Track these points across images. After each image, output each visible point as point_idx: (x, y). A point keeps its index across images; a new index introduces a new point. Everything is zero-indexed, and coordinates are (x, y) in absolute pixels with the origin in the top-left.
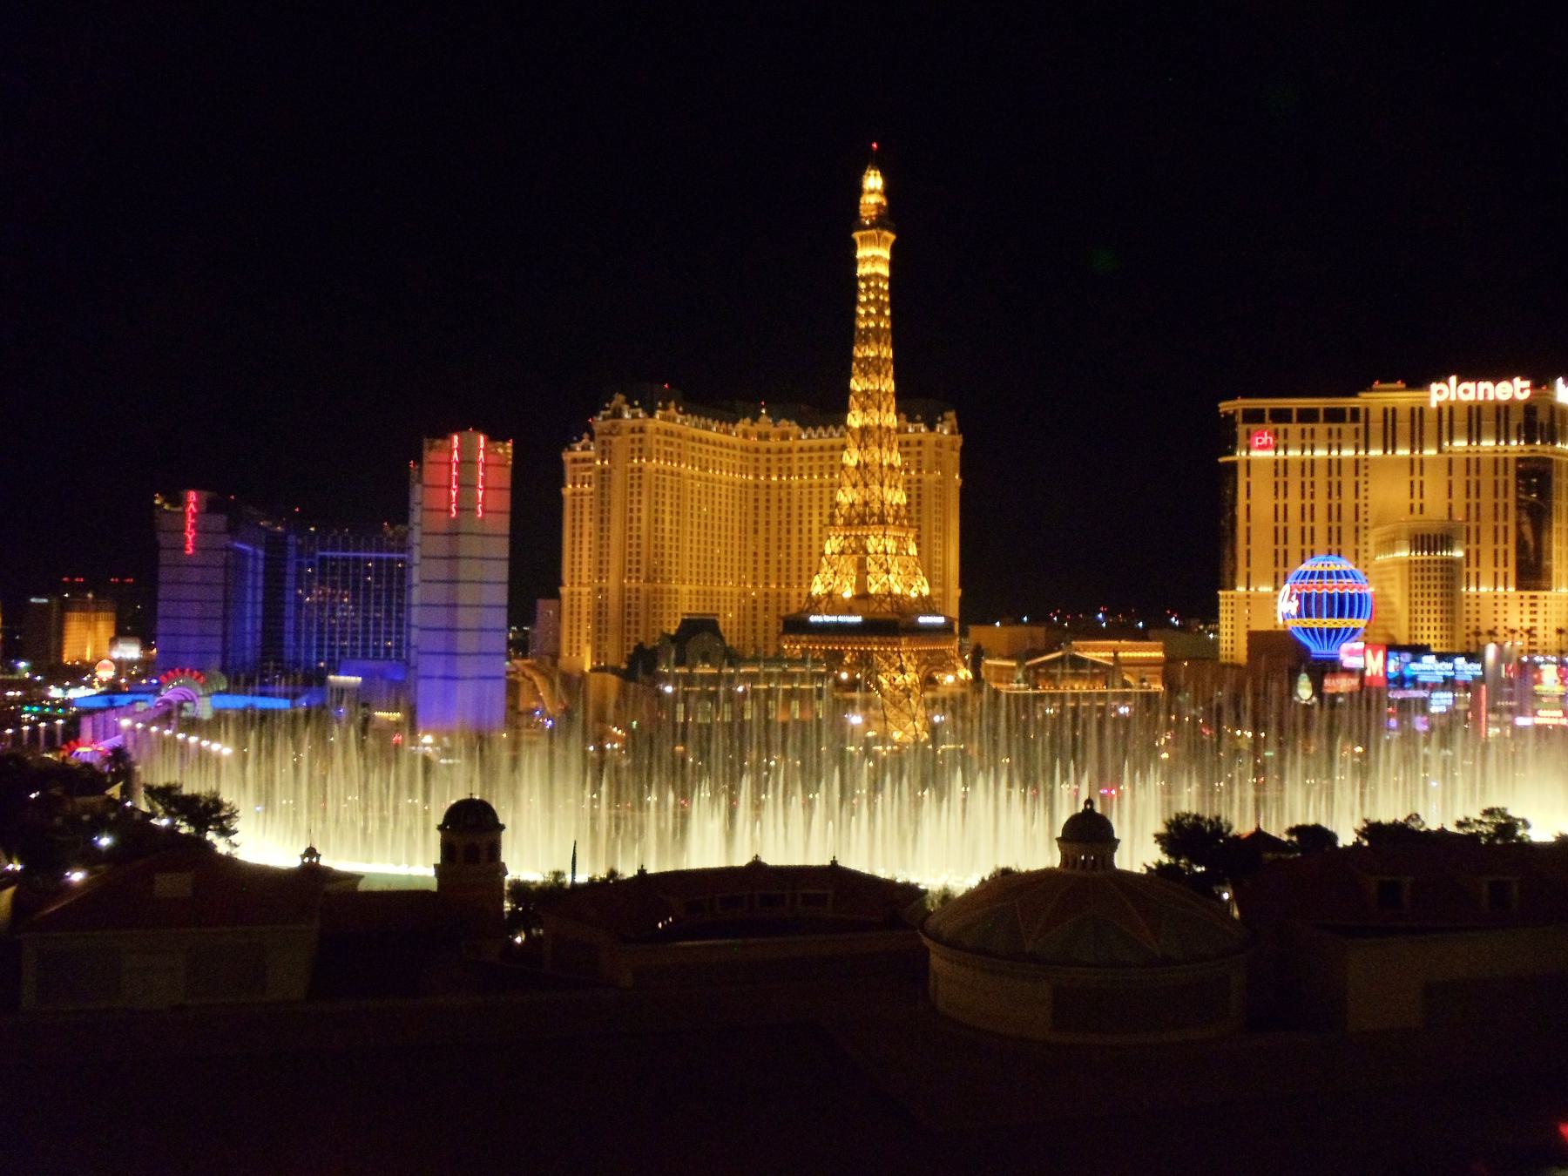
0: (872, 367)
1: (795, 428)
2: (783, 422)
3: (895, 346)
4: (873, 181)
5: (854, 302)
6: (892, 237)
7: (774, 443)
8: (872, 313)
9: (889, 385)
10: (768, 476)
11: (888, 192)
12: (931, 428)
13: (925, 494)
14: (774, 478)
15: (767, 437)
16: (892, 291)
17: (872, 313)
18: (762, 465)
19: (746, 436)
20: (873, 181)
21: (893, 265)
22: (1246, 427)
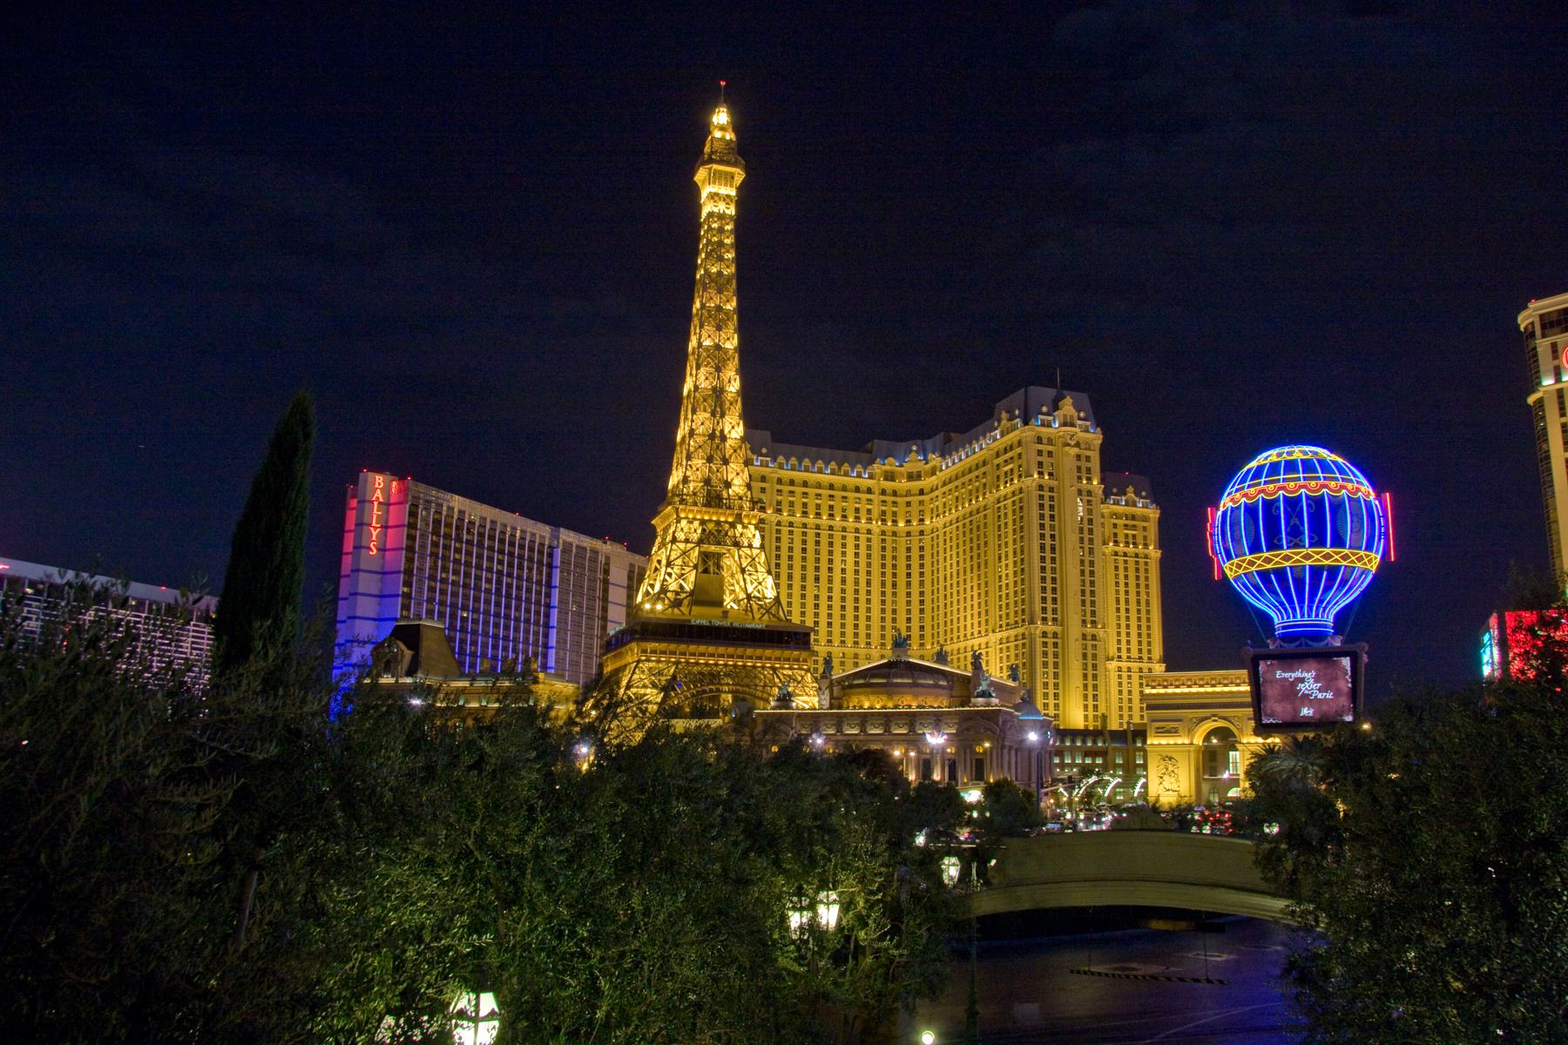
1: (935, 459)
2: (931, 456)
3: (741, 294)
4: (721, 117)
6: (739, 175)
7: (926, 483)
8: (717, 262)
10: (922, 520)
11: (737, 127)
12: (1026, 423)
13: (1025, 505)
14: (927, 522)
15: (918, 476)
16: (739, 232)
17: (717, 262)
18: (915, 509)
19: (890, 477)
20: (721, 117)
22: (1548, 341)
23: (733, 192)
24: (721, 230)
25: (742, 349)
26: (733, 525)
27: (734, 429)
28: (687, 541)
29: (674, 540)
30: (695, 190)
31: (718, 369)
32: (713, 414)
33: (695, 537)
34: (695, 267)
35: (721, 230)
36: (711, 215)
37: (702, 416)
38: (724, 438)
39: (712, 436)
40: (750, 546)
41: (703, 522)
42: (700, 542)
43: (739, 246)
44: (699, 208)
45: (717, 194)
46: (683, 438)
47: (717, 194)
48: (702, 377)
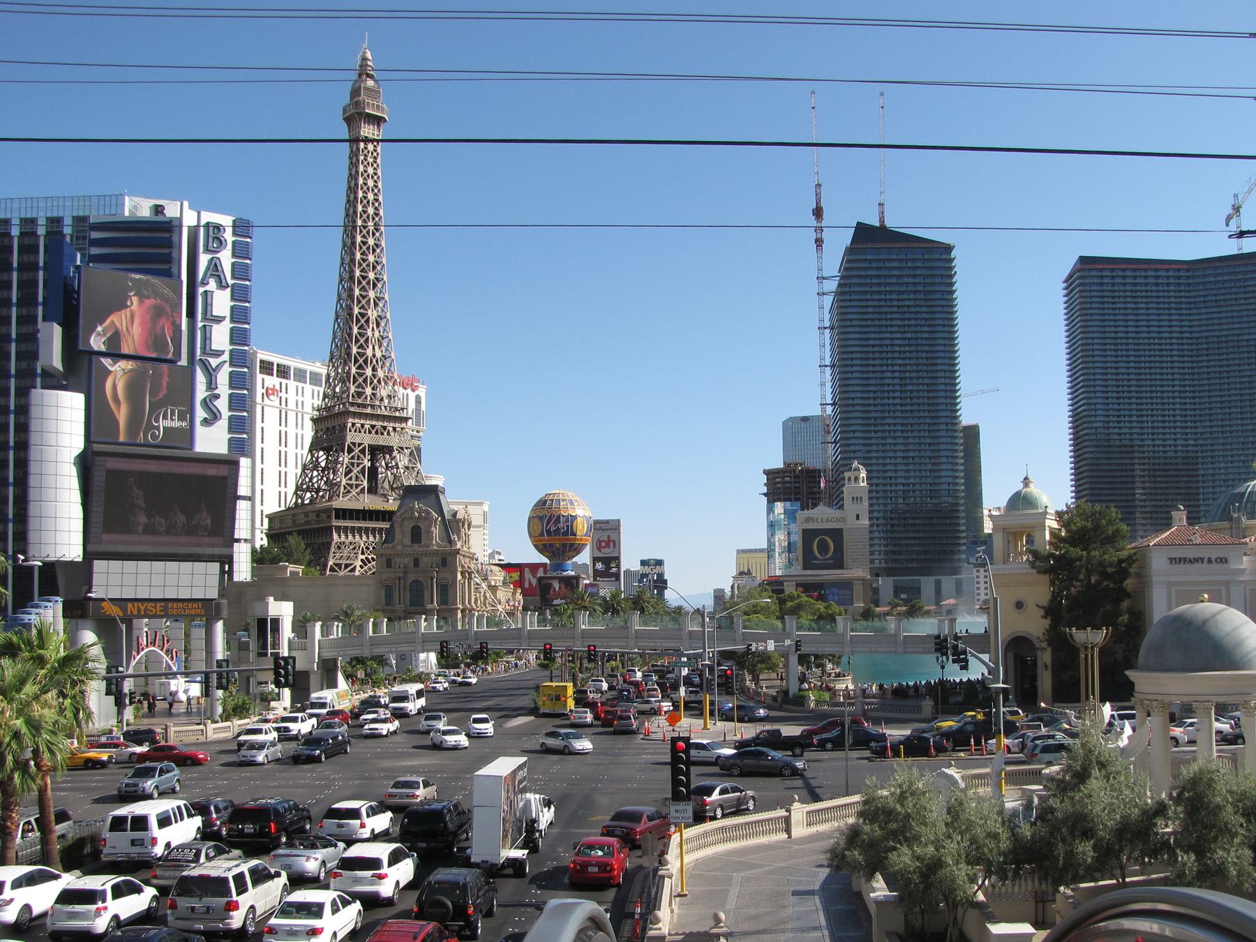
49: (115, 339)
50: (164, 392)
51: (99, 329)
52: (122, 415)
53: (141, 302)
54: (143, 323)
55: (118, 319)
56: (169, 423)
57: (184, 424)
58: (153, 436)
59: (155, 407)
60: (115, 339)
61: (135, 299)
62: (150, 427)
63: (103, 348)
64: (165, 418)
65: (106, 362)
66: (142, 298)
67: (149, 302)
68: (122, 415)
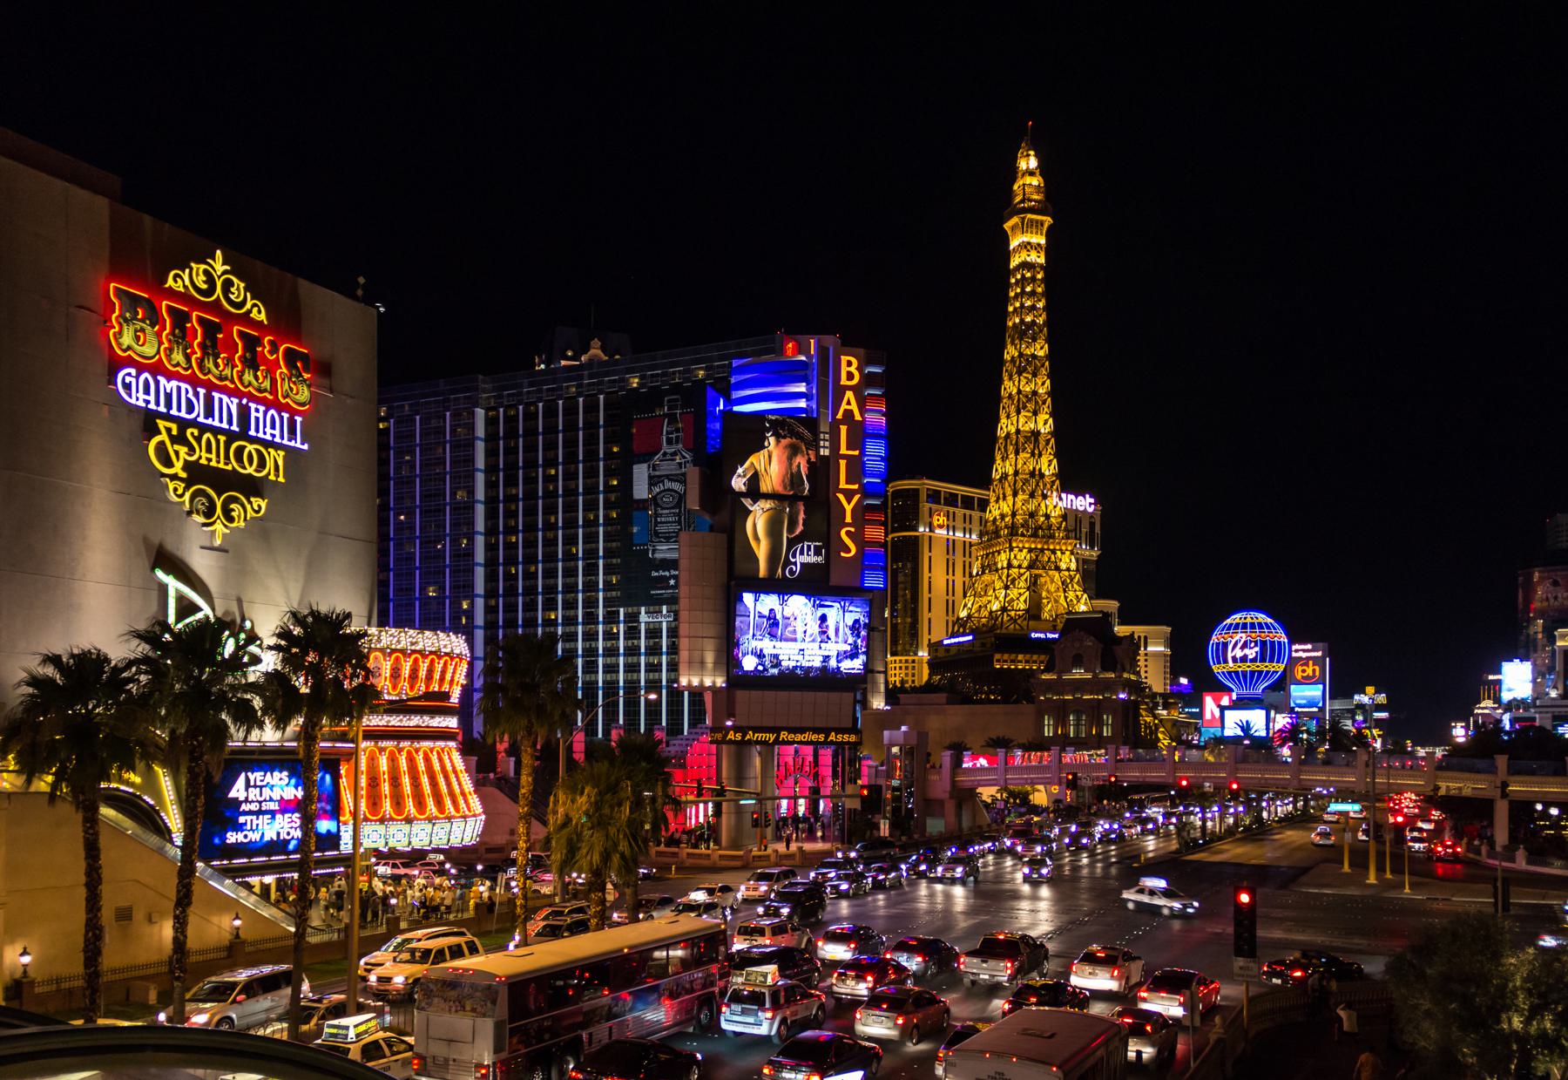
0: (1026, 365)
5: (1006, 300)
6: (1048, 220)
9: (1043, 386)
21: (1050, 250)
23: (1043, 241)
24: (1033, 279)
25: (1052, 393)
26: (1053, 551)
27: (1048, 465)
28: (1020, 567)
29: (1010, 566)
30: (1006, 240)
31: (1035, 413)
32: (1033, 454)
33: (1025, 564)
34: (1005, 314)
35: (1033, 279)
36: (1025, 265)
37: (1023, 455)
38: (1042, 476)
39: (1032, 474)
40: (1068, 569)
41: (1030, 550)
42: (1029, 568)
43: (1047, 294)
44: (1007, 255)
45: (1027, 244)
46: (1005, 476)
47: (1027, 244)
48: (1022, 420)
49: (754, 480)
50: (800, 528)
51: (740, 470)
52: (762, 551)
53: (778, 442)
54: (780, 462)
55: (757, 460)
56: (805, 559)
57: (820, 559)
58: (792, 573)
59: (791, 543)
60: (754, 480)
61: (772, 440)
62: (787, 562)
63: (744, 489)
64: (802, 553)
65: (747, 502)
66: (778, 437)
67: (785, 442)
68: (762, 551)
